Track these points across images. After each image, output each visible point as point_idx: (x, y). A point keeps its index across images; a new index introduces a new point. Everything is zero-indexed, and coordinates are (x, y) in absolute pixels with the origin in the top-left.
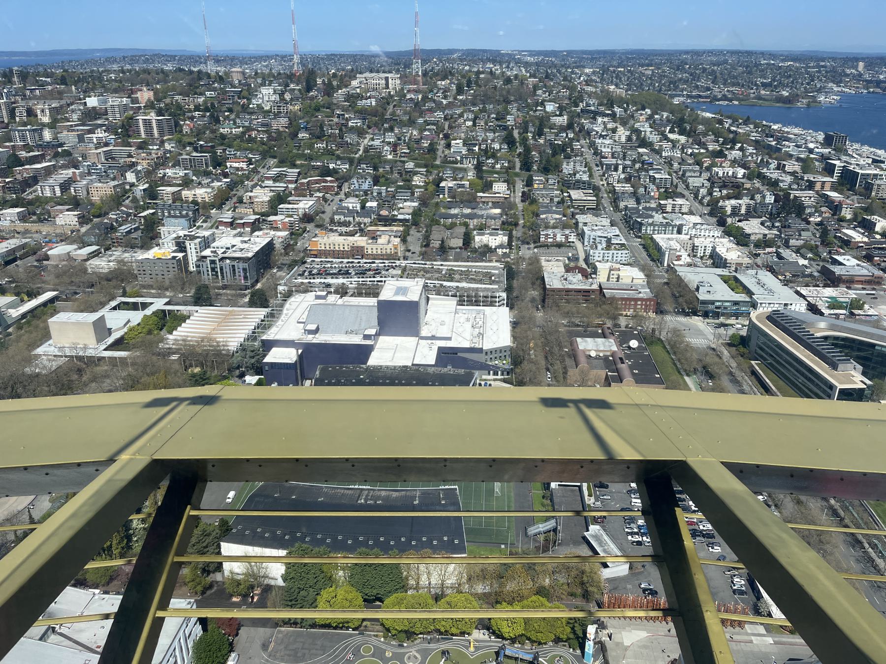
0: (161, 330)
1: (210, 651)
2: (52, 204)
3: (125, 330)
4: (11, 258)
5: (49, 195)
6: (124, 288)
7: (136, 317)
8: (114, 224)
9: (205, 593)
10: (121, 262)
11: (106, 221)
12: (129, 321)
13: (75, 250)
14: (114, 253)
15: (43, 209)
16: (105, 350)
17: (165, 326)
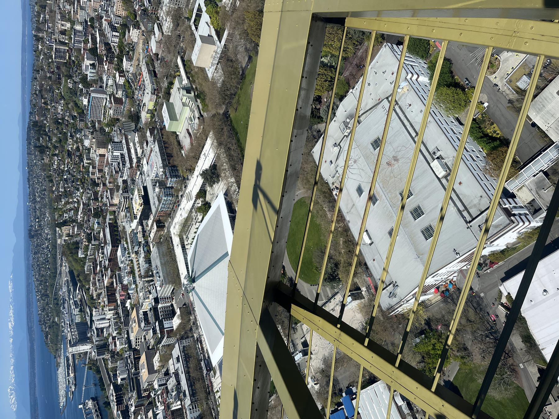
0: (217, 5)
1: (417, 46)
2: (123, 40)
3: (212, 27)
4: (153, 73)
5: (118, 40)
6: (185, 18)
7: (205, 17)
8: (142, 8)
9: (384, 38)
10: (168, 14)
11: (139, 13)
12: (207, 23)
13: (155, 37)
14: (161, 15)
15: (126, 46)
16: (220, 42)
17: (216, 2)
